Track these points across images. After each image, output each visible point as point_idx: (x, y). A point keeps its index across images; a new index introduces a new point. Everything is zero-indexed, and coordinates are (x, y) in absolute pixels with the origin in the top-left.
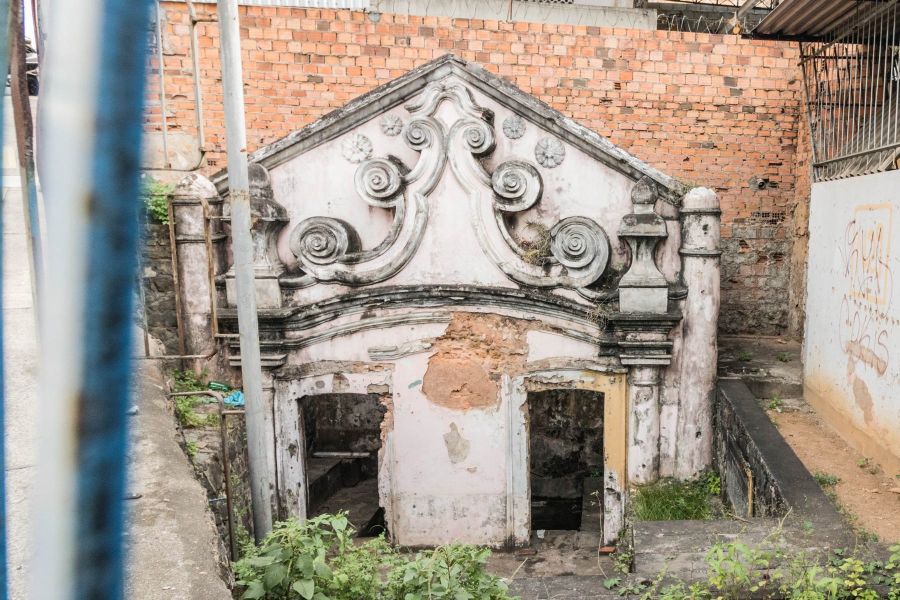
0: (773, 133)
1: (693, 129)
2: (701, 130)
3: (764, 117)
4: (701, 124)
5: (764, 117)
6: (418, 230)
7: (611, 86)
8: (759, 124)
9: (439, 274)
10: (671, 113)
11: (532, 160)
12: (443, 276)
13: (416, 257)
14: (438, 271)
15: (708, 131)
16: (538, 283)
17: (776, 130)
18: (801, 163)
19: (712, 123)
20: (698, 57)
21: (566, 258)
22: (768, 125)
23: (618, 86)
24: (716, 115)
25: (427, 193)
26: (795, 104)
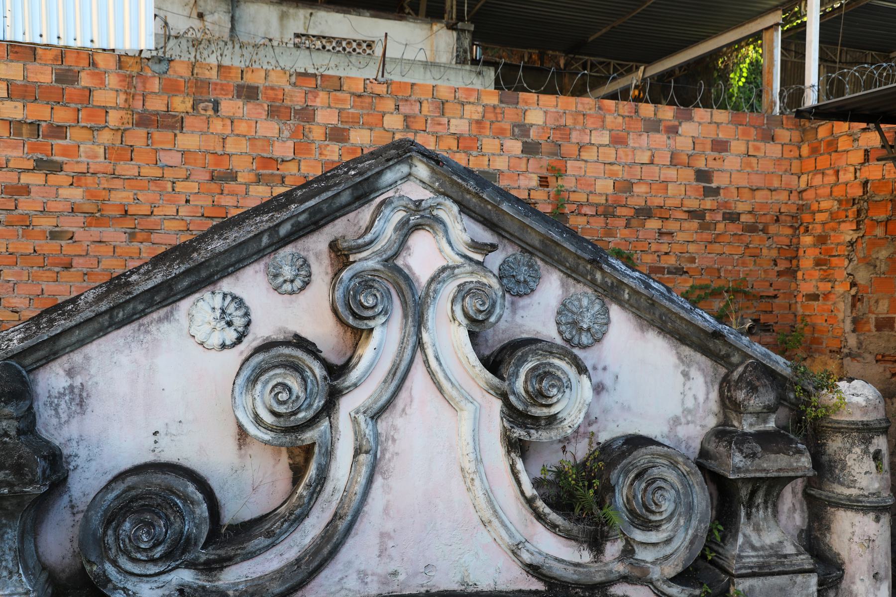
0: (765, 252)
1: (654, 247)
2: (665, 248)
3: (751, 228)
4: (665, 239)
5: (751, 228)
6: (358, 489)
7: (534, 182)
8: (747, 237)
9: (395, 574)
10: (623, 222)
11: (550, 332)
12: (401, 577)
13: (350, 542)
14: (391, 568)
15: (677, 248)
16: (584, 579)
17: (769, 248)
18: (814, 297)
19: (680, 237)
20: (660, 139)
21: (632, 523)
22: (756, 240)
23: (544, 182)
24: (686, 225)
25: (376, 416)
26: (794, 210)
